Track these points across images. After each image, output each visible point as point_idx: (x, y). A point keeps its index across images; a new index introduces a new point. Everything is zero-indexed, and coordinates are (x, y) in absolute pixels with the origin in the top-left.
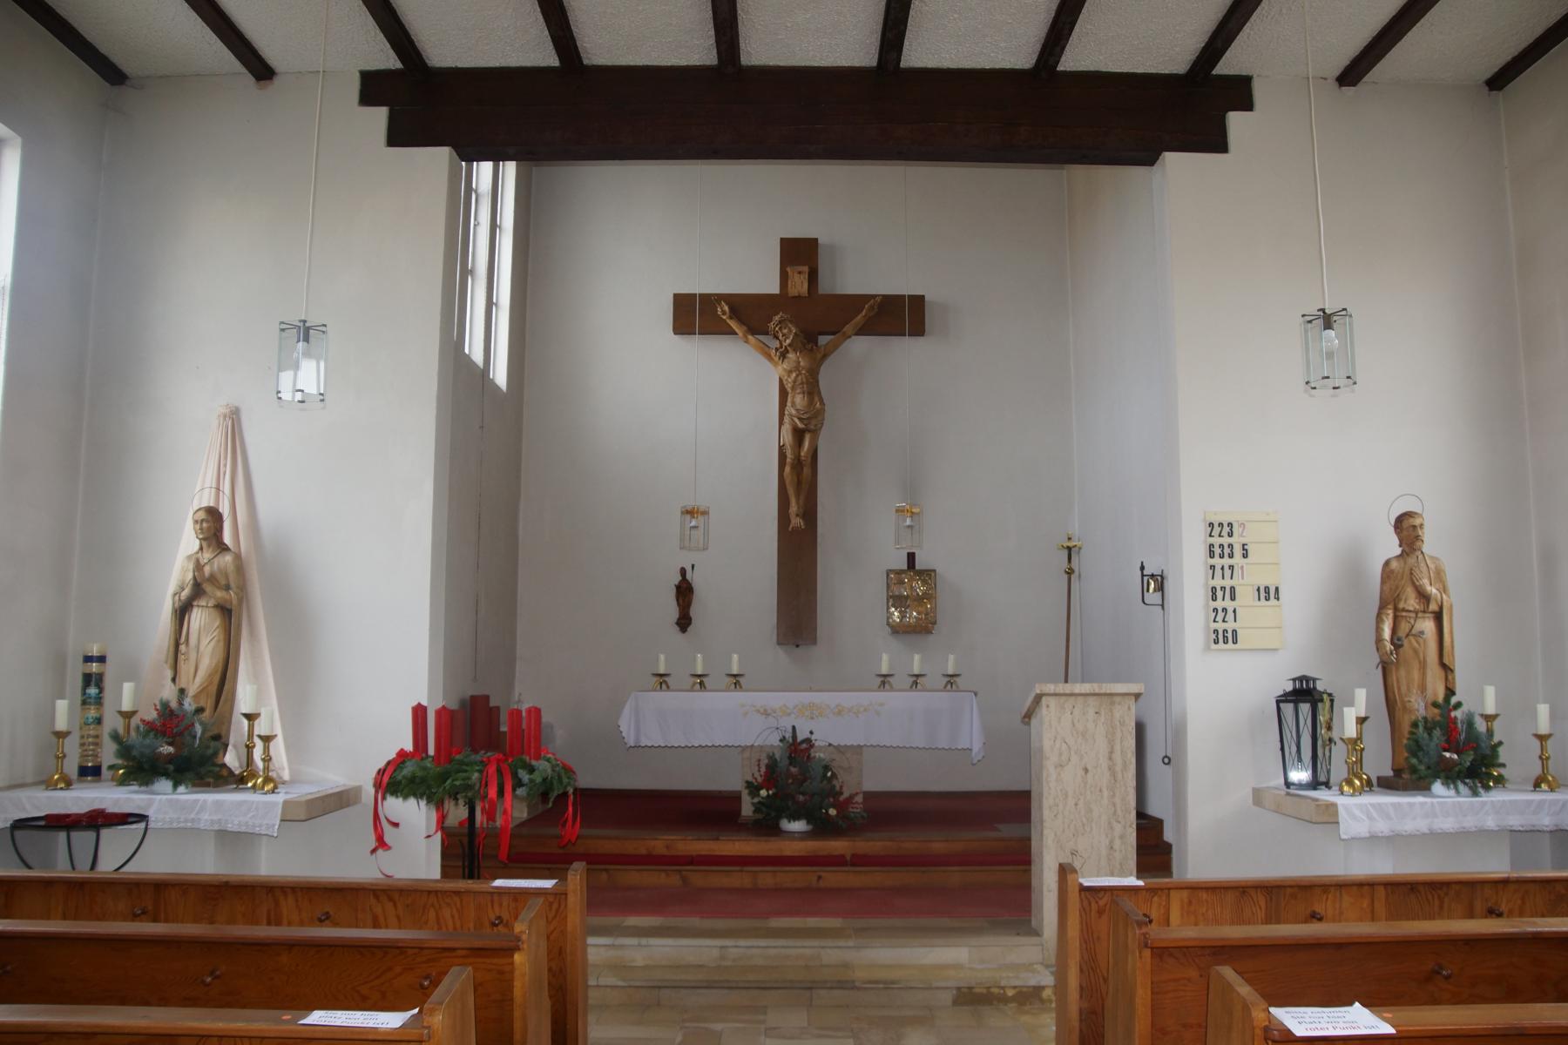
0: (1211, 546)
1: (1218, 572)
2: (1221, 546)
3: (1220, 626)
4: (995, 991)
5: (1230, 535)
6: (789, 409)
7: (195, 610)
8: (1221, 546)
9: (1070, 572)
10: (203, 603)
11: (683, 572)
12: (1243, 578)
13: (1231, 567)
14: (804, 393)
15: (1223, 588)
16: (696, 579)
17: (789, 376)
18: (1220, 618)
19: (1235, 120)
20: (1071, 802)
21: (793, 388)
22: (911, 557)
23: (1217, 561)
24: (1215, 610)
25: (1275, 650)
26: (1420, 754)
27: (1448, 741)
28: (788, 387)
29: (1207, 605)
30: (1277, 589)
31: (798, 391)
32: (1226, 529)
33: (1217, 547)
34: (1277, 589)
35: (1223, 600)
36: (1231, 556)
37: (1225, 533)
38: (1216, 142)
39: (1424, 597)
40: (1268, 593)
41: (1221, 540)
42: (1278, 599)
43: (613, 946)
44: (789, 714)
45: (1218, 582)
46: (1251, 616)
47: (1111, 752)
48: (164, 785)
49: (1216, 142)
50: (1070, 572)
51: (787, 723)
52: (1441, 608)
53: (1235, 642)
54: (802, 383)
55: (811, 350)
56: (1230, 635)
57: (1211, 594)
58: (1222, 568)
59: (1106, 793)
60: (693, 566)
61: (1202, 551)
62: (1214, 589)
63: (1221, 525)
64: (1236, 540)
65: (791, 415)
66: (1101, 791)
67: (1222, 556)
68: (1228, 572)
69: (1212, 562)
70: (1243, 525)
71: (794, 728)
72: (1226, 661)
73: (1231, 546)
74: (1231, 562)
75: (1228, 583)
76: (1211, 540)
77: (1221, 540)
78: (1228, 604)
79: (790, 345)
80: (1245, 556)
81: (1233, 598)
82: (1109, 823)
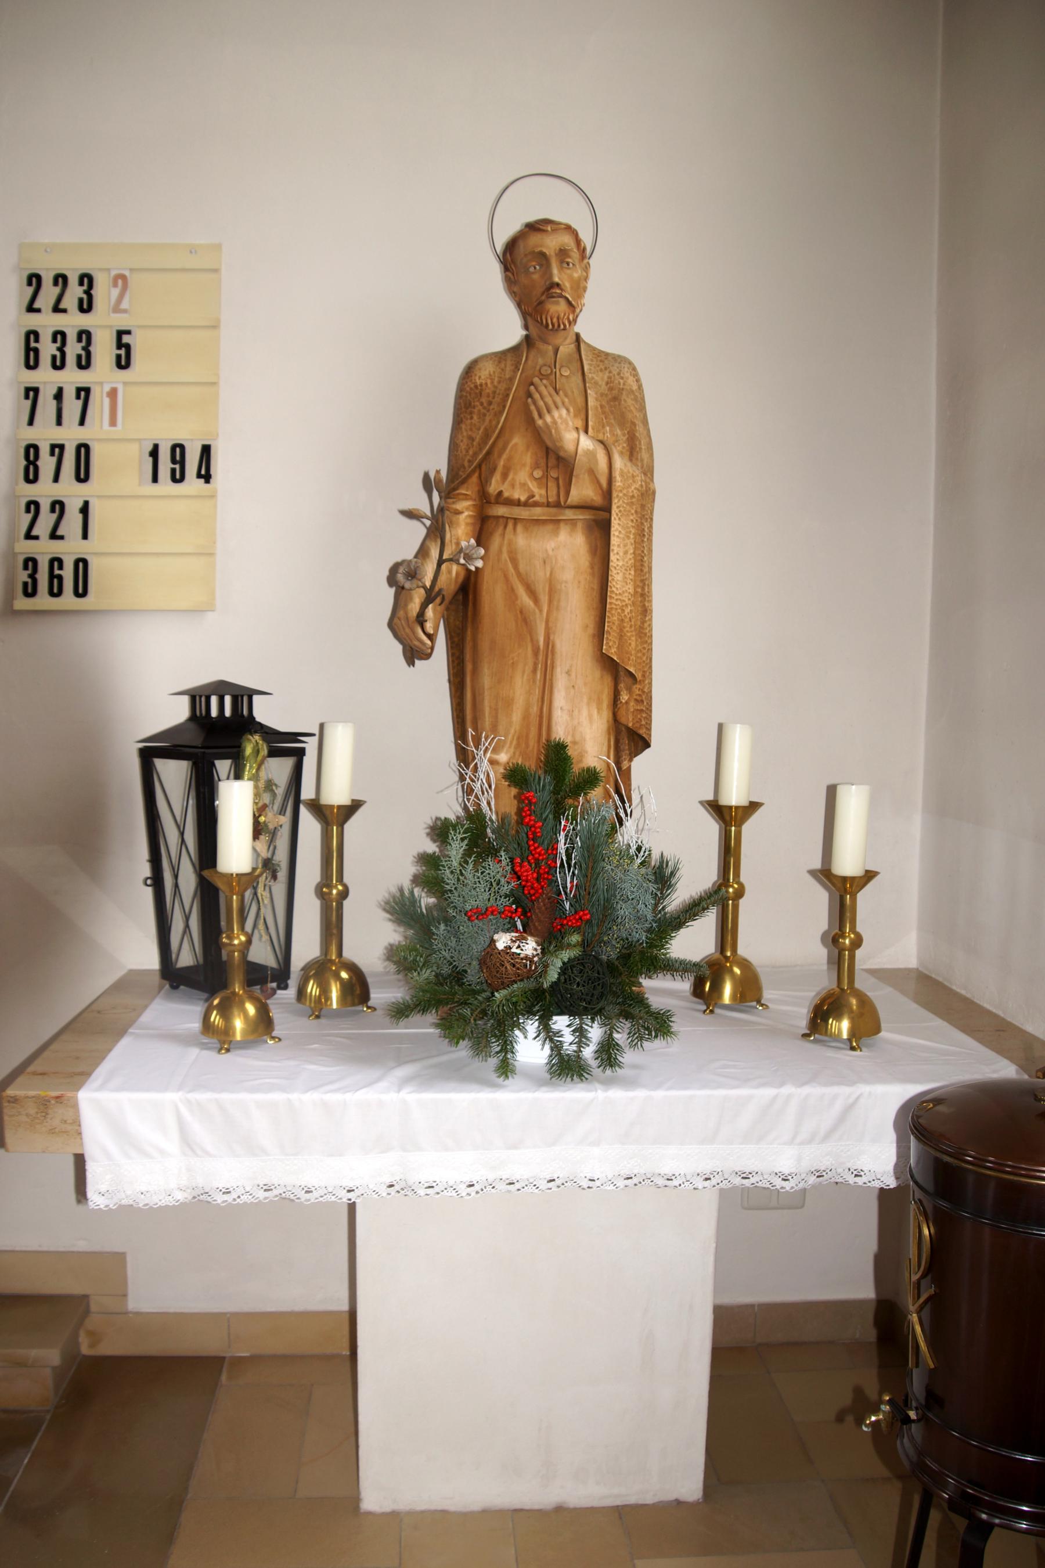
0: (32, 335)
1: (47, 406)
2: (59, 336)
5: (86, 306)
8: (59, 336)
12: (113, 422)
13: (84, 393)
15: (57, 449)
18: (43, 527)
23: (45, 377)
32: (75, 292)
33: (46, 337)
34: (206, 450)
35: (56, 479)
36: (84, 363)
37: (70, 301)
41: (59, 322)
42: (207, 478)
45: (45, 433)
53: (81, 592)
56: (67, 573)
57: (24, 463)
58: (59, 396)
62: (32, 452)
63: (61, 279)
67: (58, 364)
68: (72, 407)
70: (121, 280)
73: (85, 336)
74: (83, 378)
75: (70, 435)
76: (33, 321)
77: (59, 322)
78: (71, 492)
80: (123, 362)
81: (83, 475)
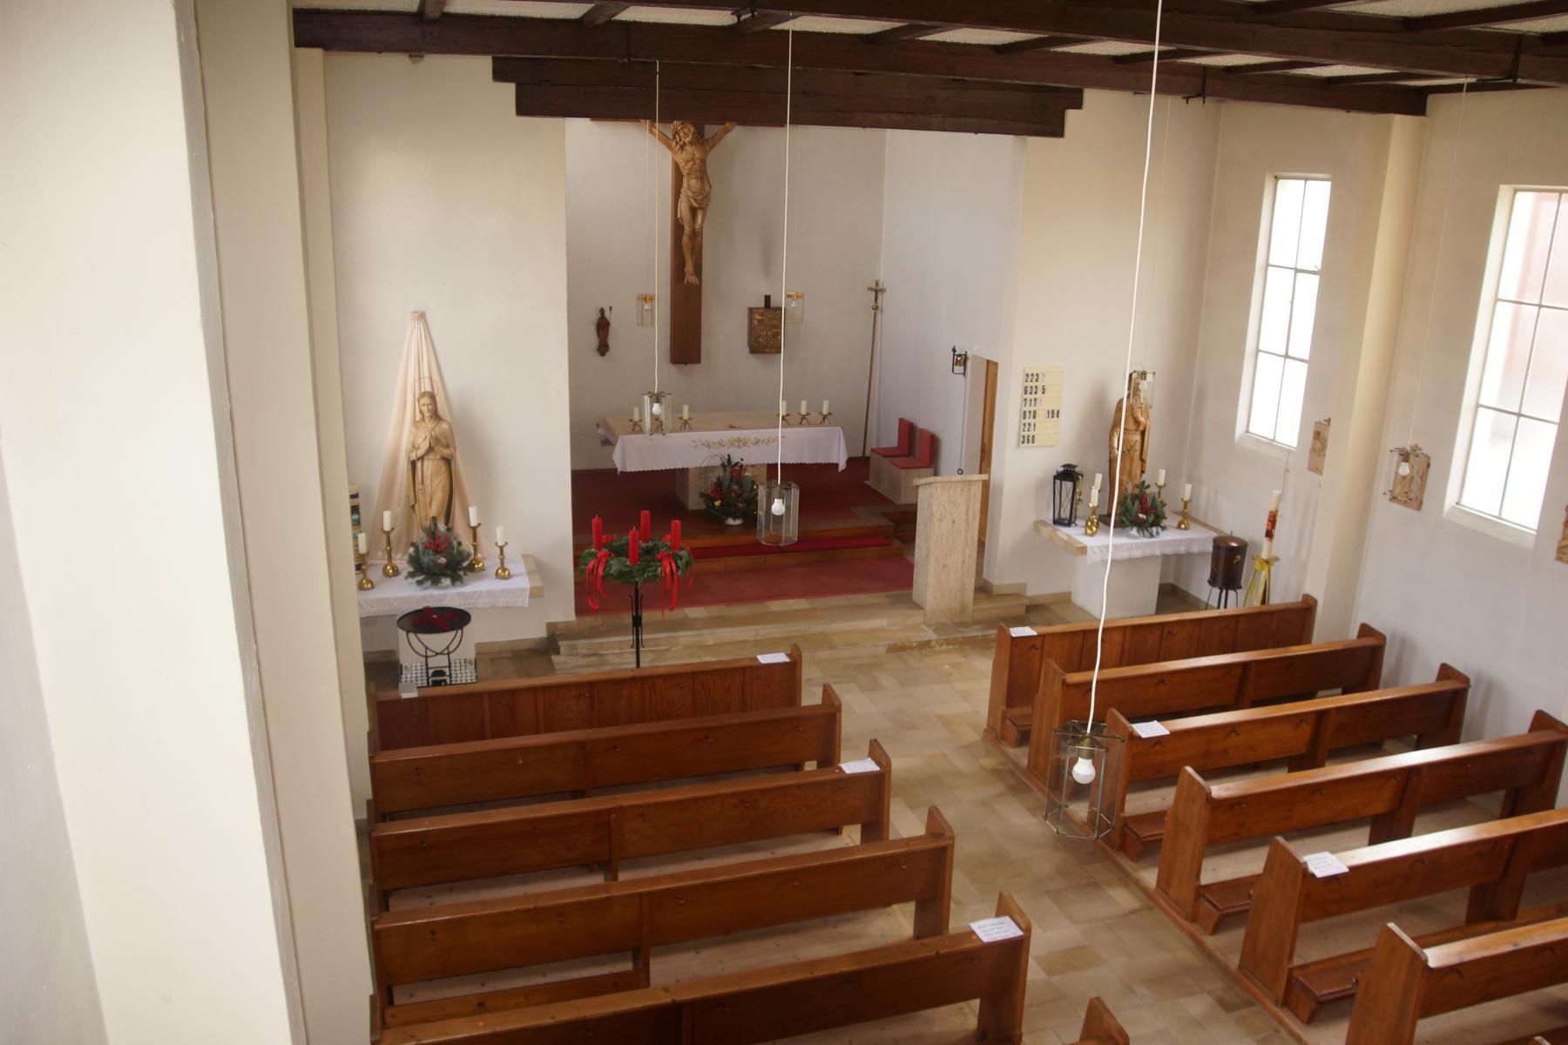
2: (1031, 387)
3: (1026, 433)
4: (907, 644)
5: (1037, 381)
6: (684, 190)
7: (426, 462)
8: (1031, 387)
9: (876, 308)
10: (431, 456)
11: (602, 311)
13: (1035, 399)
14: (696, 178)
15: (1030, 412)
16: (612, 317)
17: (686, 165)
19: (1071, 114)
20: (945, 539)
21: (689, 174)
22: (767, 299)
23: (1028, 396)
24: (1025, 424)
25: (1053, 446)
26: (1127, 515)
27: (1142, 508)
28: (685, 172)
29: (1020, 421)
30: (1058, 412)
31: (693, 176)
32: (1035, 377)
34: (1058, 412)
38: (1056, 130)
39: (1137, 423)
40: (1054, 414)
41: (1031, 384)
42: (1058, 416)
43: (697, 635)
44: (724, 446)
45: (1027, 408)
46: (1044, 427)
47: (968, 511)
48: (446, 581)
49: (1056, 130)
50: (876, 308)
51: (725, 451)
52: (1145, 429)
53: (1033, 442)
54: (696, 171)
55: (703, 143)
59: (963, 533)
60: (611, 308)
61: (1021, 390)
63: (1032, 375)
64: (1039, 384)
65: (688, 197)
66: (961, 532)
68: (1033, 402)
69: (1025, 396)
70: (1044, 375)
71: (729, 456)
72: (1028, 452)
73: (1036, 387)
74: (1036, 396)
75: (1032, 409)
76: (1026, 384)
77: (1031, 384)
78: (1032, 421)
79: (689, 142)
80: (1043, 393)
81: (1034, 417)
82: (964, 550)
